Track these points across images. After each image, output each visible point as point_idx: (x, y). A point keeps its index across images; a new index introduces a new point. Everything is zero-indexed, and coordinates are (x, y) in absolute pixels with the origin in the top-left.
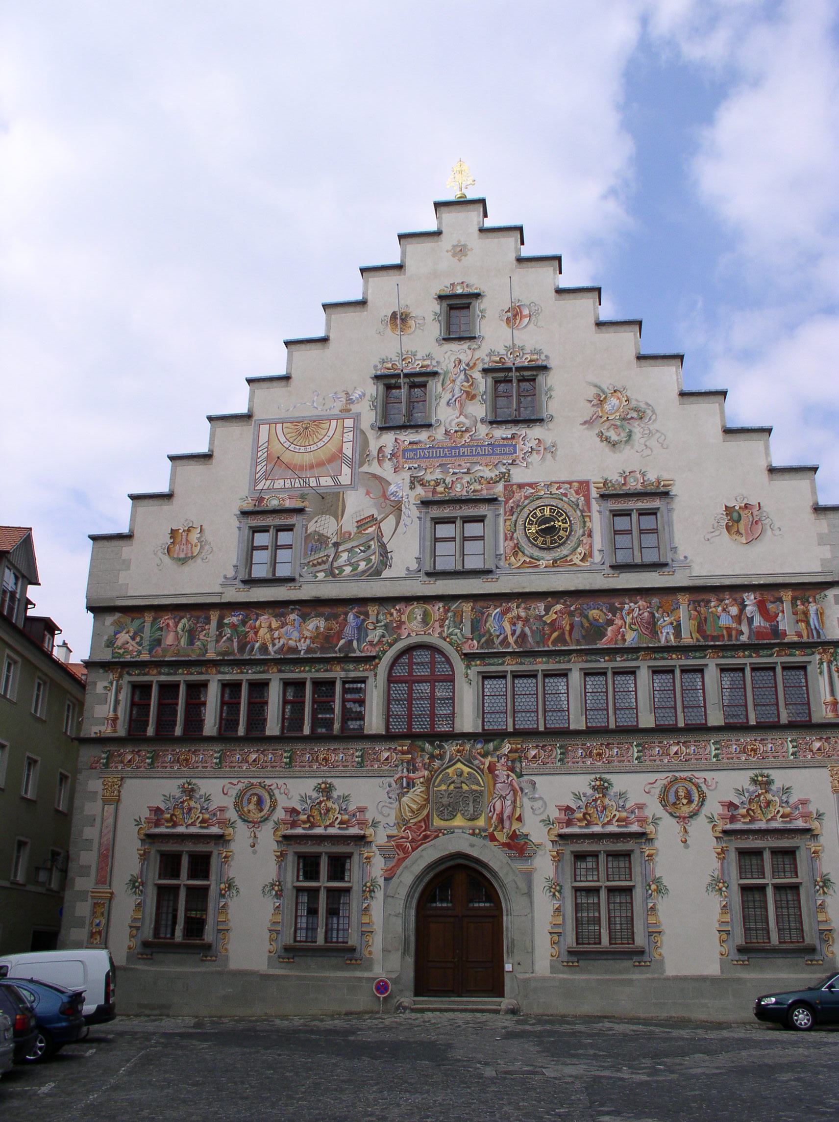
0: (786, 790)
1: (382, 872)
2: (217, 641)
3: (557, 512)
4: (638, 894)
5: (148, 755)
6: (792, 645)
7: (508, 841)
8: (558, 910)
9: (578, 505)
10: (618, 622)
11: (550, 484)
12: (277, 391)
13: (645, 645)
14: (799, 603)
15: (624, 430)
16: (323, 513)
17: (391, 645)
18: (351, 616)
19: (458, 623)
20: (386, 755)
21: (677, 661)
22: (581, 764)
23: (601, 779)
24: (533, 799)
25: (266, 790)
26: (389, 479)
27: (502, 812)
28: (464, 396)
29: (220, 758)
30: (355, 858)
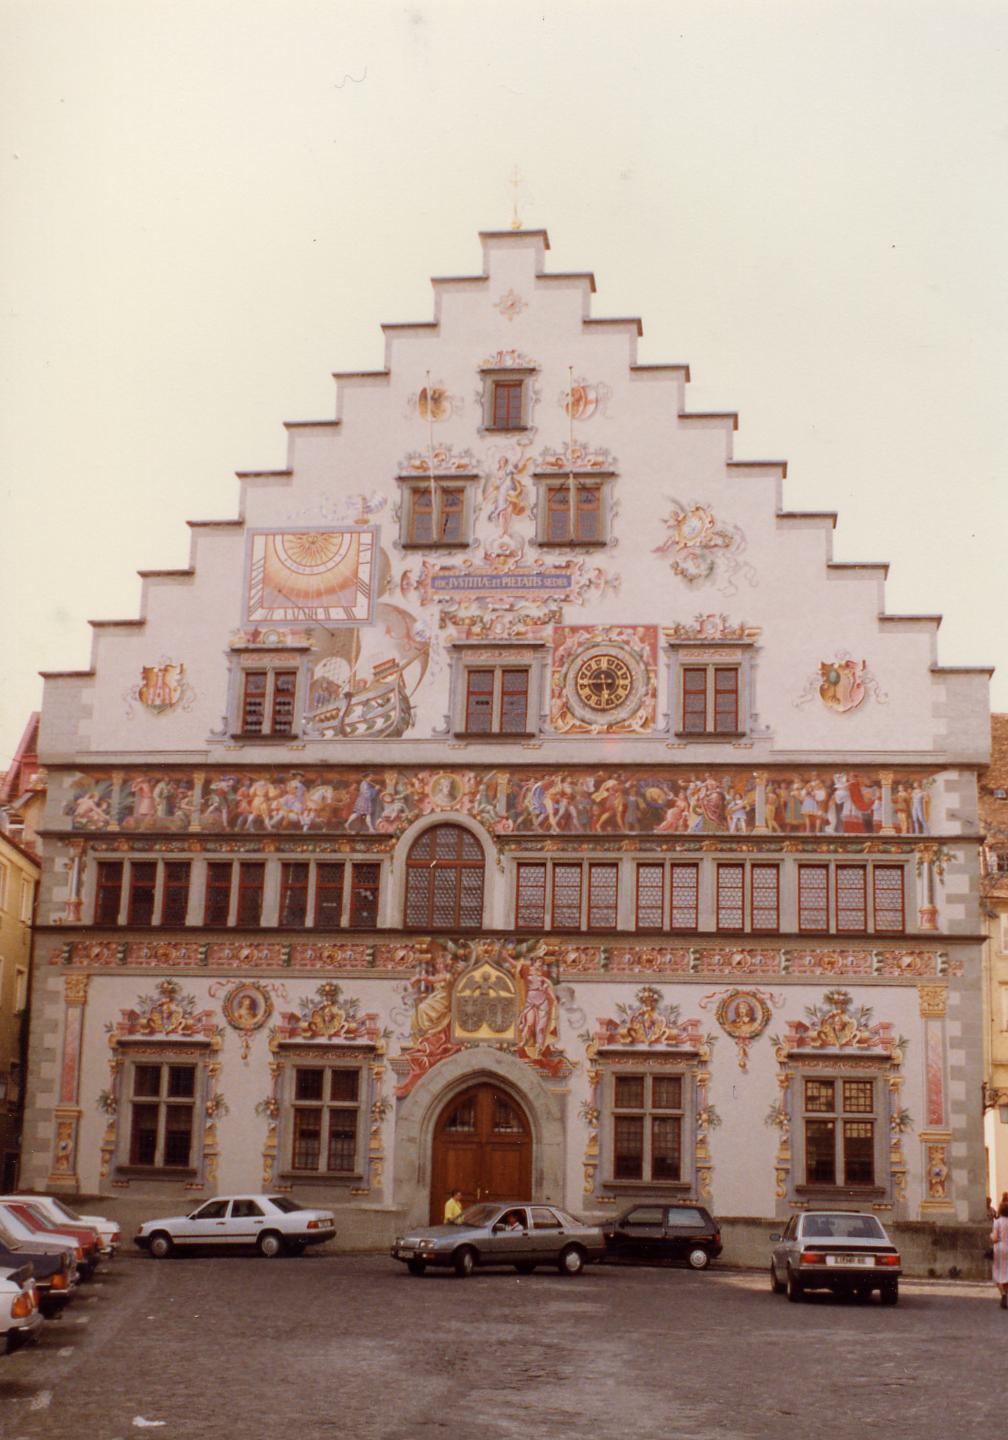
0: (866, 1012)
1: (394, 1091)
2: (202, 811)
3: (620, 664)
4: (687, 1125)
5: (120, 948)
6: (887, 840)
7: (540, 1057)
8: (594, 1139)
9: (641, 657)
10: (681, 803)
11: (611, 628)
12: (274, 490)
13: (711, 833)
14: (901, 788)
15: (705, 561)
16: (333, 655)
17: (411, 822)
18: (364, 786)
19: (491, 798)
20: (401, 953)
21: (747, 854)
22: (627, 972)
23: (650, 990)
24: (570, 1010)
25: (261, 992)
26: (414, 614)
27: (534, 1025)
28: (510, 509)
29: (205, 953)
30: (364, 1074)
